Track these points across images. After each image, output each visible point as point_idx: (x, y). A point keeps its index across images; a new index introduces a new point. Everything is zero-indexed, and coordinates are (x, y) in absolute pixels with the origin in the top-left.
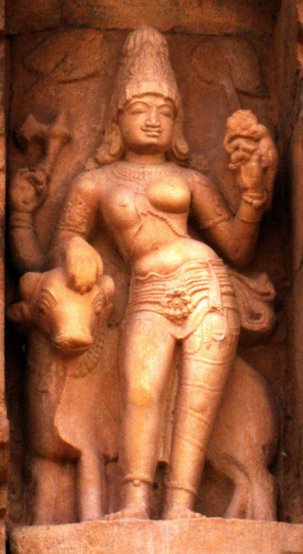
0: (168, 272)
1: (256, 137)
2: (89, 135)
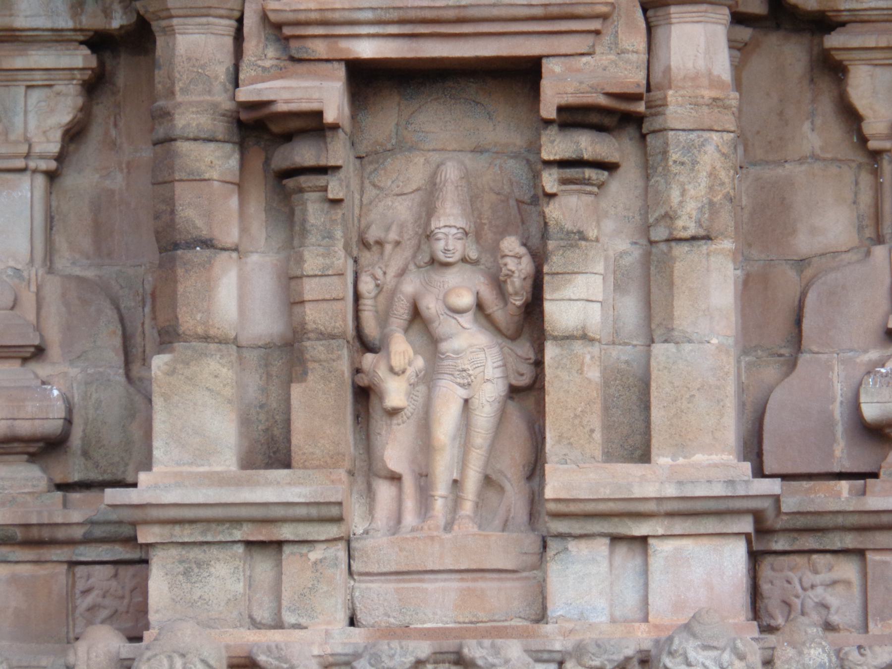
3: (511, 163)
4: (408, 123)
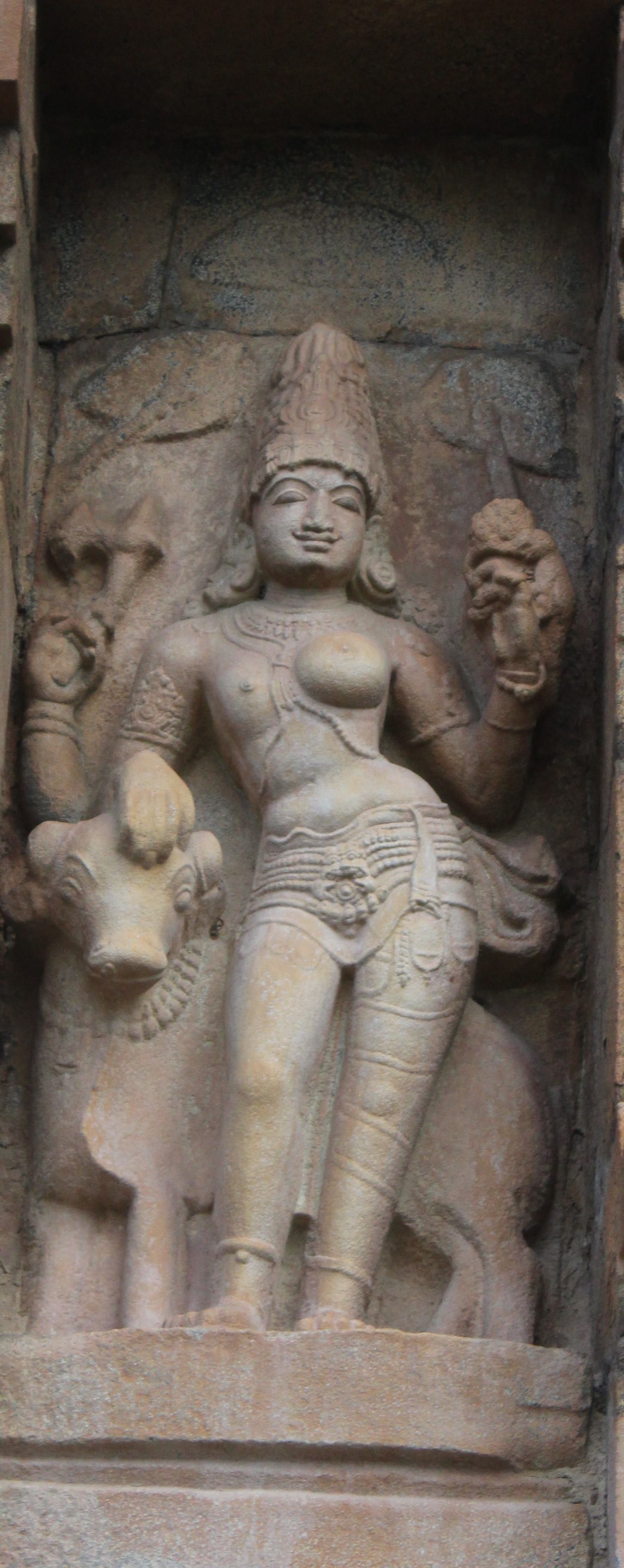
0: (331, 825)
1: (528, 556)
2: (198, 549)
3: (497, 367)
4: (197, 260)
